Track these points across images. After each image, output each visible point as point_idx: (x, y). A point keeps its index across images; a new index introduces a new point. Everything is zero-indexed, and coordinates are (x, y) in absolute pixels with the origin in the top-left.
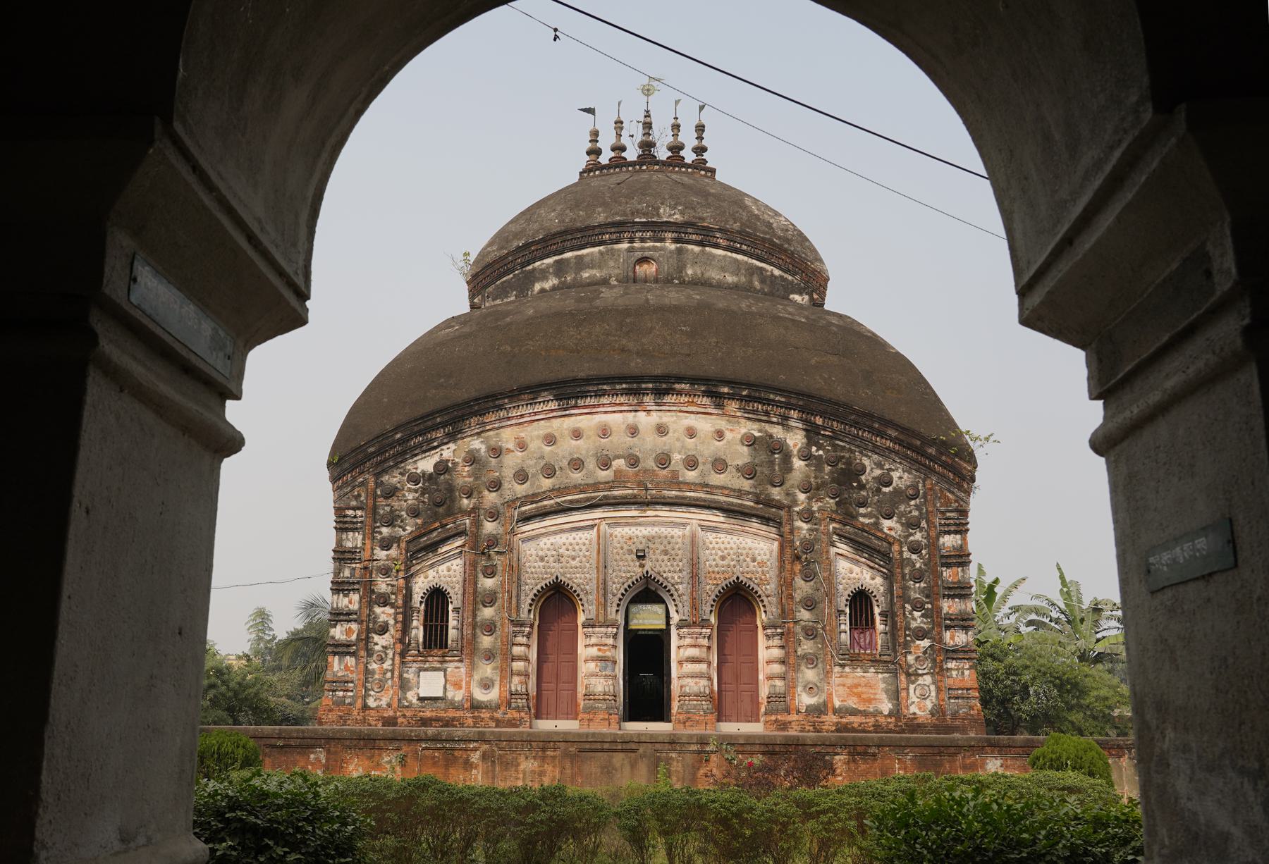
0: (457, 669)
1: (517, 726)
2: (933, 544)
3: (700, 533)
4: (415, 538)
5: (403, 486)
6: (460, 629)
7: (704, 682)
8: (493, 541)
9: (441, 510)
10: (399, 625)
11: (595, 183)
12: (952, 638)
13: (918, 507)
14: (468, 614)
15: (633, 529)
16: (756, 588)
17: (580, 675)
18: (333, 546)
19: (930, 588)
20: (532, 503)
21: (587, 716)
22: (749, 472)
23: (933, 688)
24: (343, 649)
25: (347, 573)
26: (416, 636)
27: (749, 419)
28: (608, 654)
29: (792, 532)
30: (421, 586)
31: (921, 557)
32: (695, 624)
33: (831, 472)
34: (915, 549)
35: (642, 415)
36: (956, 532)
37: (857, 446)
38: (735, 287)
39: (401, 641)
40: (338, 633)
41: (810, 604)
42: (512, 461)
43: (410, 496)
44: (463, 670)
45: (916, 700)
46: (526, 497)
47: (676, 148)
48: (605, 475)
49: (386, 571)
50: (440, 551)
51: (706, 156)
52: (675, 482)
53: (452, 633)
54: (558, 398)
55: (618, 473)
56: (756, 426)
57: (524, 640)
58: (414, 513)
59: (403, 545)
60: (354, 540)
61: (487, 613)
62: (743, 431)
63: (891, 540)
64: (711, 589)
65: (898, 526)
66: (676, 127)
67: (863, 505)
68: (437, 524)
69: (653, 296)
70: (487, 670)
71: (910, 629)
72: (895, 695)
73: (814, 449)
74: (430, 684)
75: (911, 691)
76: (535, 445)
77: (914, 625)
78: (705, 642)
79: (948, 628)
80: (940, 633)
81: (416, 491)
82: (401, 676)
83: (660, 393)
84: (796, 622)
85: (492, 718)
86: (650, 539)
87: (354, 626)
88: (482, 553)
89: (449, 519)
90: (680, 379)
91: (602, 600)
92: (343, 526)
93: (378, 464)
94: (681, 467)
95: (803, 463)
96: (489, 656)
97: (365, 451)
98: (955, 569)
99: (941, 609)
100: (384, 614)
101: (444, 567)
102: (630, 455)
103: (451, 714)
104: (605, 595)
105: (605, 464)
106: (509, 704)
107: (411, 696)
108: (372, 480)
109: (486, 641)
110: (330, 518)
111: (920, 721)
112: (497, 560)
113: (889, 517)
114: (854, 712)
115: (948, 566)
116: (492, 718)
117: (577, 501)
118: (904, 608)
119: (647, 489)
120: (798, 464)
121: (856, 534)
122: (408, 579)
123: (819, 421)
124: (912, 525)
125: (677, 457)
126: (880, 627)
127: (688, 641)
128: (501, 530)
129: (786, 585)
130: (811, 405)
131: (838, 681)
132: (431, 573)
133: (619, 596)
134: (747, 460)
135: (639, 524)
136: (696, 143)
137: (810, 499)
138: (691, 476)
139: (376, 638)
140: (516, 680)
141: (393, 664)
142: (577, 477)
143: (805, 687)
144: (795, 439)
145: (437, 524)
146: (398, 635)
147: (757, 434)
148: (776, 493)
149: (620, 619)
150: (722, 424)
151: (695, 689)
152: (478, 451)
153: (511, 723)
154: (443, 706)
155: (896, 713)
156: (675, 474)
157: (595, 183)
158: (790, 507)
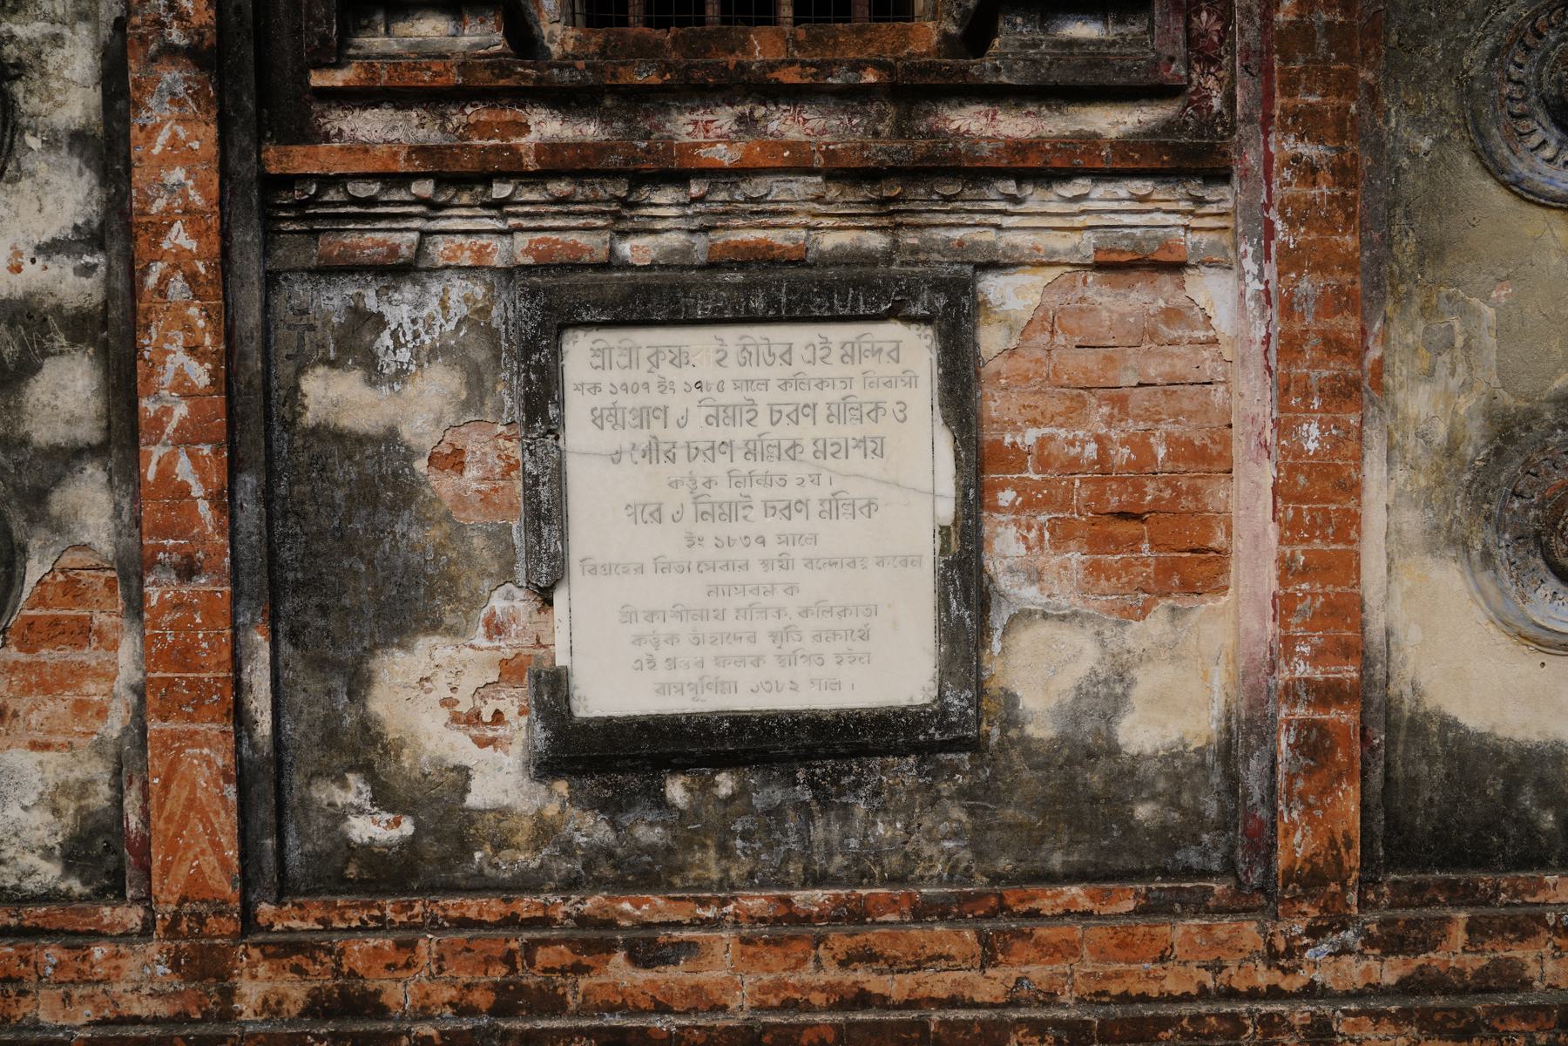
44: (1223, 299)
82: (252, 411)
141: (116, 230)
154: (940, 839)
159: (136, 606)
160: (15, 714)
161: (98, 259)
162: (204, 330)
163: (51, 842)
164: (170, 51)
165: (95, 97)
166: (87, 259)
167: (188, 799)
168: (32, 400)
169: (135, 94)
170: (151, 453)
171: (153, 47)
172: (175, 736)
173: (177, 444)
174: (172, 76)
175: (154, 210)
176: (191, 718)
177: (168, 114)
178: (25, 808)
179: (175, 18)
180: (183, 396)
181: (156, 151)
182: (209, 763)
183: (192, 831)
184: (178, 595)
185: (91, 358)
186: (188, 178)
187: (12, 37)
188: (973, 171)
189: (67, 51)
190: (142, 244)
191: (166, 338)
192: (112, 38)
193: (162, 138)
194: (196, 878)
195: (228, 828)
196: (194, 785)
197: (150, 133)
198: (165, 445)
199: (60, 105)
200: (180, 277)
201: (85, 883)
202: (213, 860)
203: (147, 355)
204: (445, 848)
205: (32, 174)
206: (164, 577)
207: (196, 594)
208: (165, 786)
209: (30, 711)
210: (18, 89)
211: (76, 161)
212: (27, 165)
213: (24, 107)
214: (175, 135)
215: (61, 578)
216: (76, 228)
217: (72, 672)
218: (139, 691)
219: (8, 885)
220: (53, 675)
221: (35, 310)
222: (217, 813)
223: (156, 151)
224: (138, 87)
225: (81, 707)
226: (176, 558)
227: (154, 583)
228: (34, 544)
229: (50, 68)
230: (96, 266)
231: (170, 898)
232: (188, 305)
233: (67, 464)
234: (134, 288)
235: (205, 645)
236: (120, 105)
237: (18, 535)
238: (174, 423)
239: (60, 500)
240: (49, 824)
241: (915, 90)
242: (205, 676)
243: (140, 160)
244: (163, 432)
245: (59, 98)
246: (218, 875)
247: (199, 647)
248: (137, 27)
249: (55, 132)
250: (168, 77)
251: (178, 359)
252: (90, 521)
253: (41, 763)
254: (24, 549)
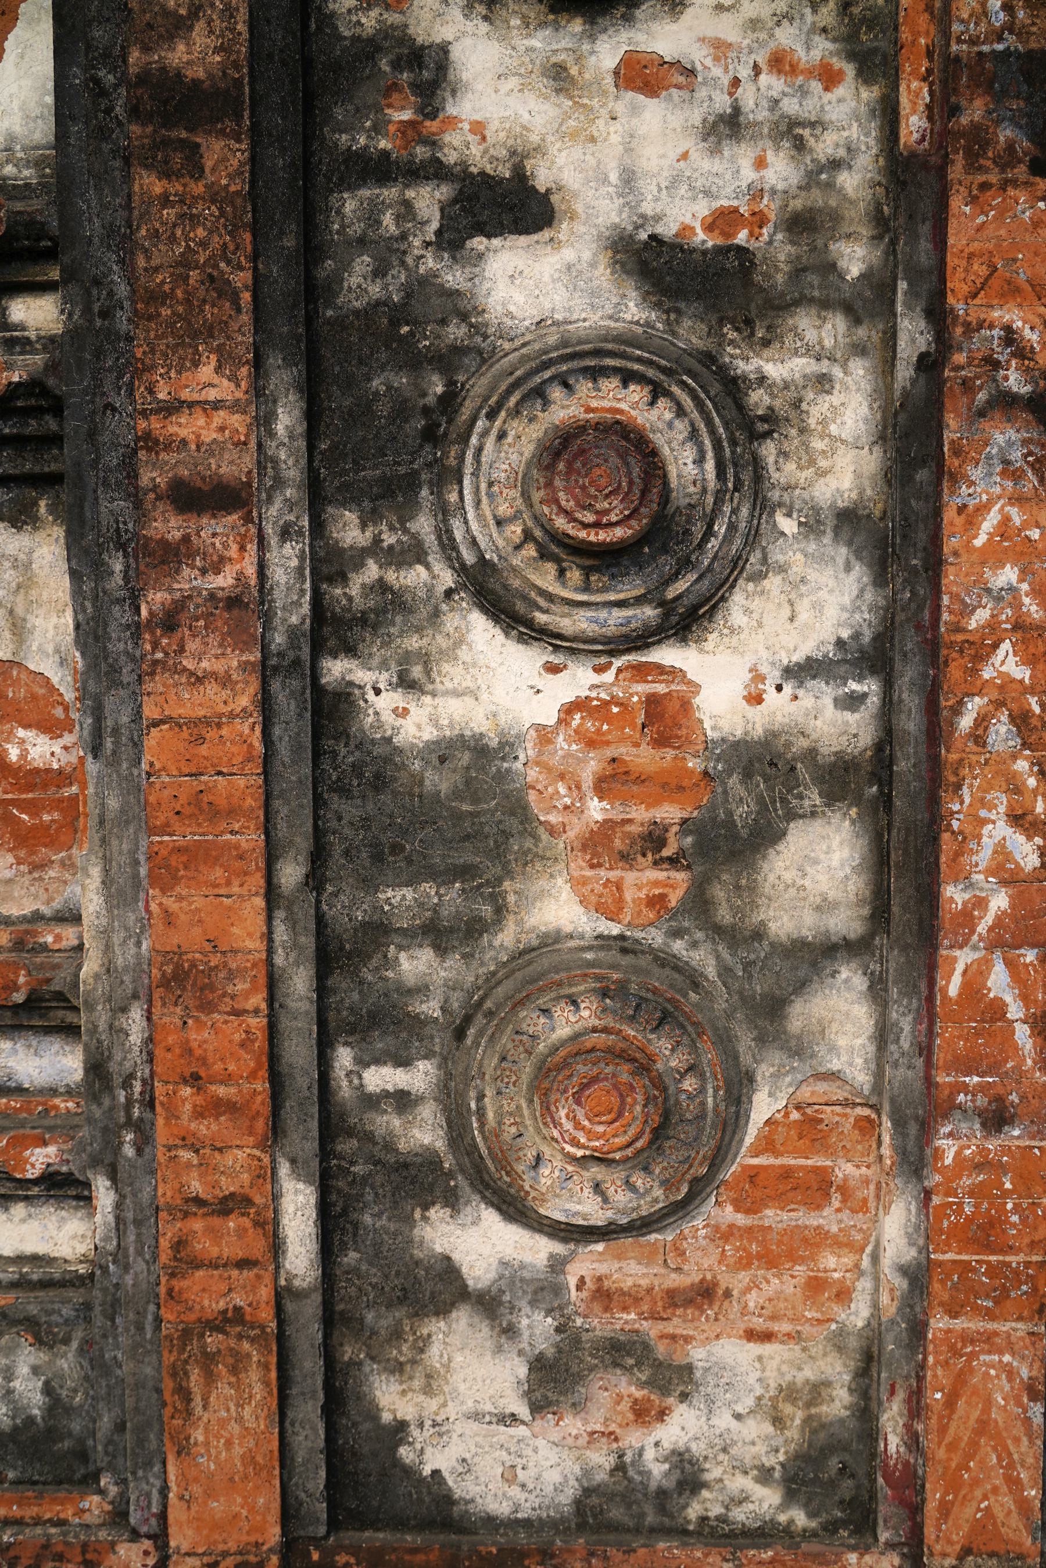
159: (915, 1161)
160: (728, 1294)
161: (871, 686)
162: (1035, 792)
163: (770, 1461)
164: (1005, 403)
165: (871, 461)
166: (854, 686)
167: (979, 1421)
168: (771, 878)
169: (952, 462)
170: (955, 960)
171: (982, 396)
172: (967, 1338)
173: (990, 948)
174: (1006, 437)
175: (973, 625)
176: (990, 1315)
177: (997, 490)
178: (738, 1417)
179: (1013, 355)
180: (1003, 883)
181: (978, 542)
182: (1011, 1373)
183: (982, 1461)
184: (983, 1151)
185: (853, 822)
186: (1021, 580)
187: (762, 379)
189: (835, 399)
190: (955, 672)
191: (983, 803)
192: (914, 381)
193: (989, 524)
194: (985, 1525)
195: (1030, 1460)
196: (988, 1402)
197: (972, 517)
198: (975, 948)
199: (823, 473)
200: (1004, 718)
201: (811, 1515)
202: (1008, 1501)
203: (955, 825)
205: (782, 569)
206: (964, 1127)
207: (1006, 1150)
208: (950, 1402)
209: (748, 1289)
210: (768, 451)
211: (843, 550)
212: (777, 556)
213: (775, 475)
214: (1006, 520)
215: (795, 1115)
216: (840, 643)
217: (805, 1240)
218: (918, 1277)
219: (711, 1515)
220: (779, 1243)
221: (780, 756)
222: (1017, 1440)
223: (978, 542)
224: (957, 452)
225: (816, 1286)
226: (981, 1101)
227: (950, 1135)
228: (764, 1071)
229: (812, 422)
230: (865, 695)
231: (949, 1550)
232: (1014, 757)
233: (814, 964)
234: (936, 728)
235: (1015, 1218)
236: (922, 475)
237: (746, 1059)
238: (989, 919)
239: (801, 1014)
240: (767, 1438)
242: (1013, 1259)
243: (956, 554)
244: (973, 931)
245: (823, 463)
246: (1015, 1521)
247: (1007, 1221)
248: (958, 368)
249: (816, 510)
250: (1000, 439)
251: (998, 830)
252: (842, 1042)
253: (760, 1358)
254: (750, 1078)
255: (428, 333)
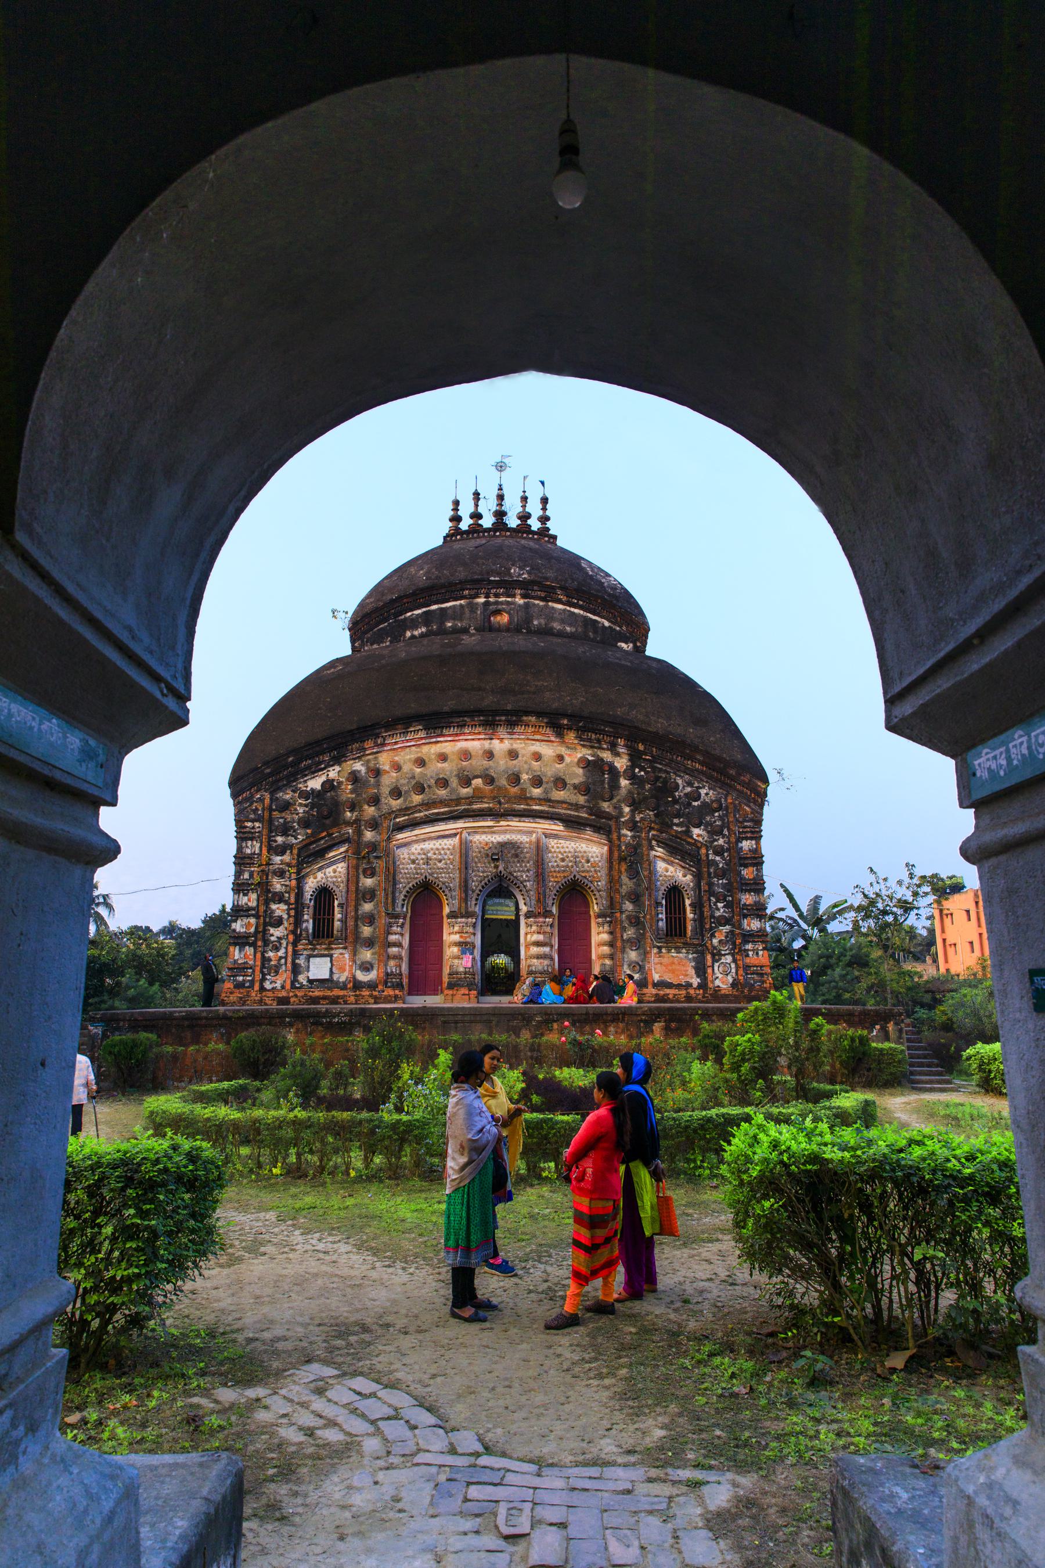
0: (342, 955)
1: (390, 1002)
2: (733, 848)
3: (543, 839)
4: (304, 847)
5: (295, 801)
6: (343, 921)
7: (546, 962)
8: (373, 846)
9: (327, 822)
10: (292, 920)
11: (457, 546)
12: (749, 925)
13: (721, 818)
14: (351, 908)
15: (489, 837)
16: (590, 884)
17: (446, 957)
18: (235, 852)
19: (730, 883)
20: (404, 815)
21: (451, 992)
22: (584, 789)
23: (733, 965)
24: (241, 941)
25: (246, 876)
26: (307, 928)
27: (584, 746)
28: (468, 940)
29: (619, 839)
30: (311, 884)
31: (723, 858)
32: (539, 915)
33: (650, 790)
34: (719, 852)
35: (496, 742)
36: (751, 839)
37: (671, 768)
38: (571, 636)
39: (294, 932)
40: (238, 926)
41: (635, 897)
42: (388, 780)
43: (301, 810)
44: (347, 956)
45: (720, 976)
46: (400, 810)
47: (524, 517)
48: (465, 791)
49: (281, 874)
50: (327, 856)
51: (549, 524)
52: (523, 797)
53: (337, 924)
54: (426, 728)
55: (477, 789)
56: (589, 752)
57: (399, 929)
58: (305, 823)
59: (295, 851)
60: (253, 847)
61: (367, 907)
62: (579, 755)
63: (699, 845)
64: (553, 883)
65: (704, 833)
66: (524, 499)
67: (678, 816)
68: (324, 834)
69: (504, 642)
70: (367, 955)
71: (714, 917)
72: (701, 970)
73: (637, 770)
74: (319, 968)
75: (716, 968)
76: (406, 768)
77: (717, 914)
78: (548, 929)
79: (745, 916)
80: (739, 922)
81: (306, 806)
82: (294, 964)
83: (512, 724)
84: (622, 912)
85: (371, 996)
86: (503, 845)
87: (253, 920)
88: (365, 857)
89: (335, 830)
90: (527, 713)
91: (463, 895)
92: (243, 835)
93: (273, 783)
94: (528, 785)
95: (627, 782)
96: (370, 943)
97: (263, 769)
98: (751, 869)
99: (740, 900)
100: (279, 909)
101: (330, 869)
102: (487, 775)
103: (337, 992)
104: (466, 891)
105: (466, 782)
106: (386, 983)
107: (302, 978)
108: (267, 796)
109: (366, 931)
110: (232, 828)
111: (723, 992)
112: (376, 863)
113: (698, 826)
114: (670, 986)
115: (746, 866)
116: (371, 996)
117: (443, 813)
118: (710, 900)
119: (500, 803)
120: (624, 782)
121: (671, 840)
122: (300, 880)
123: (641, 747)
124: (714, 832)
125: (525, 777)
126: (690, 915)
127: (534, 928)
128: (378, 838)
129: (613, 882)
130: (635, 736)
131: (657, 960)
132: (320, 875)
133: (477, 892)
134: (582, 779)
135: (494, 832)
136: (541, 513)
137: (633, 812)
138: (537, 792)
139: (272, 930)
140: (392, 963)
141: (286, 952)
142: (442, 793)
143: (629, 965)
144: (621, 763)
145: (324, 834)
146: (291, 928)
147: (590, 758)
148: (606, 806)
149: (477, 909)
150: (563, 750)
151: (540, 968)
152: (359, 772)
153: (387, 1000)
155: (703, 986)
156: (523, 790)
157: (457, 546)
158: (617, 818)
188: (332, 949)
204: (302, 986)
241: (330, 943)
255: (269, 940)
